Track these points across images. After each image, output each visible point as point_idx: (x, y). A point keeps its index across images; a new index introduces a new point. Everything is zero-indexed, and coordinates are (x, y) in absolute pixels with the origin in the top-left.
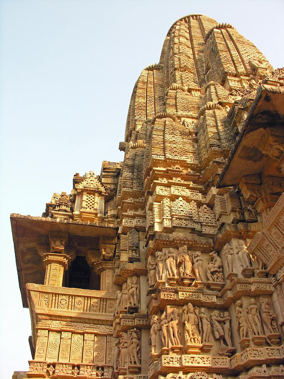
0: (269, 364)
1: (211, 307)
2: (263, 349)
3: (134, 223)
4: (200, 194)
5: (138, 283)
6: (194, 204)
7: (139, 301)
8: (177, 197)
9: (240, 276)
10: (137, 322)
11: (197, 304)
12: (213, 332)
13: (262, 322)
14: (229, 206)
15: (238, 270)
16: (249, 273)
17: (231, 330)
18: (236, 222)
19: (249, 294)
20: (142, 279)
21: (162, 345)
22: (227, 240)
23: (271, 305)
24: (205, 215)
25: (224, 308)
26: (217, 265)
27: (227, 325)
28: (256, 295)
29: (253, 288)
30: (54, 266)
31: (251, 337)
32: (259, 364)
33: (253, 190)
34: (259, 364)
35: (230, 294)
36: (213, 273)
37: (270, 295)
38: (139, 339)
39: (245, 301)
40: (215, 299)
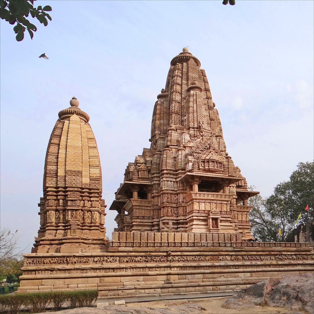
0: (183, 220)
1: (174, 207)
2: (183, 217)
3: (157, 182)
4: (175, 179)
5: (158, 198)
6: (173, 182)
7: (158, 203)
8: (169, 181)
9: (181, 203)
10: (158, 208)
11: (171, 207)
12: (174, 212)
13: (184, 212)
14: (181, 185)
15: (181, 201)
16: (183, 202)
17: (178, 212)
18: (182, 190)
19: (182, 206)
20: (159, 197)
21: (164, 215)
22: (179, 193)
23: (186, 209)
24: (175, 185)
25: (177, 208)
26: (177, 198)
27: (177, 211)
28: (183, 206)
29: (183, 205)
30: (135, 192)
31: (181, 215)
32: (182, 219)
33: (186, 183)
34: (182, 219)
35: (178, 206)
36: (175, 200)
37: (187, 207)
38: (158, 211)
39: (181, 208)
40: (175, 206)
